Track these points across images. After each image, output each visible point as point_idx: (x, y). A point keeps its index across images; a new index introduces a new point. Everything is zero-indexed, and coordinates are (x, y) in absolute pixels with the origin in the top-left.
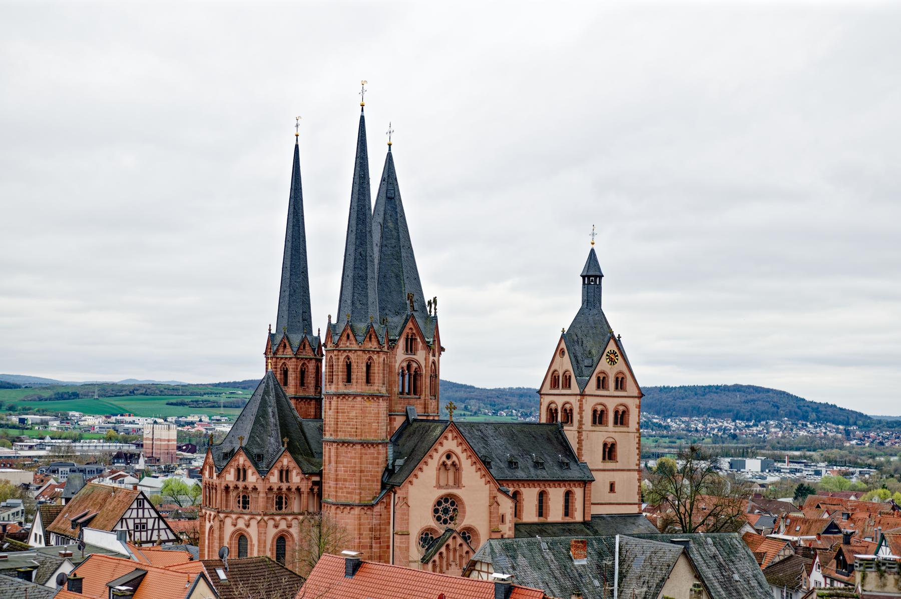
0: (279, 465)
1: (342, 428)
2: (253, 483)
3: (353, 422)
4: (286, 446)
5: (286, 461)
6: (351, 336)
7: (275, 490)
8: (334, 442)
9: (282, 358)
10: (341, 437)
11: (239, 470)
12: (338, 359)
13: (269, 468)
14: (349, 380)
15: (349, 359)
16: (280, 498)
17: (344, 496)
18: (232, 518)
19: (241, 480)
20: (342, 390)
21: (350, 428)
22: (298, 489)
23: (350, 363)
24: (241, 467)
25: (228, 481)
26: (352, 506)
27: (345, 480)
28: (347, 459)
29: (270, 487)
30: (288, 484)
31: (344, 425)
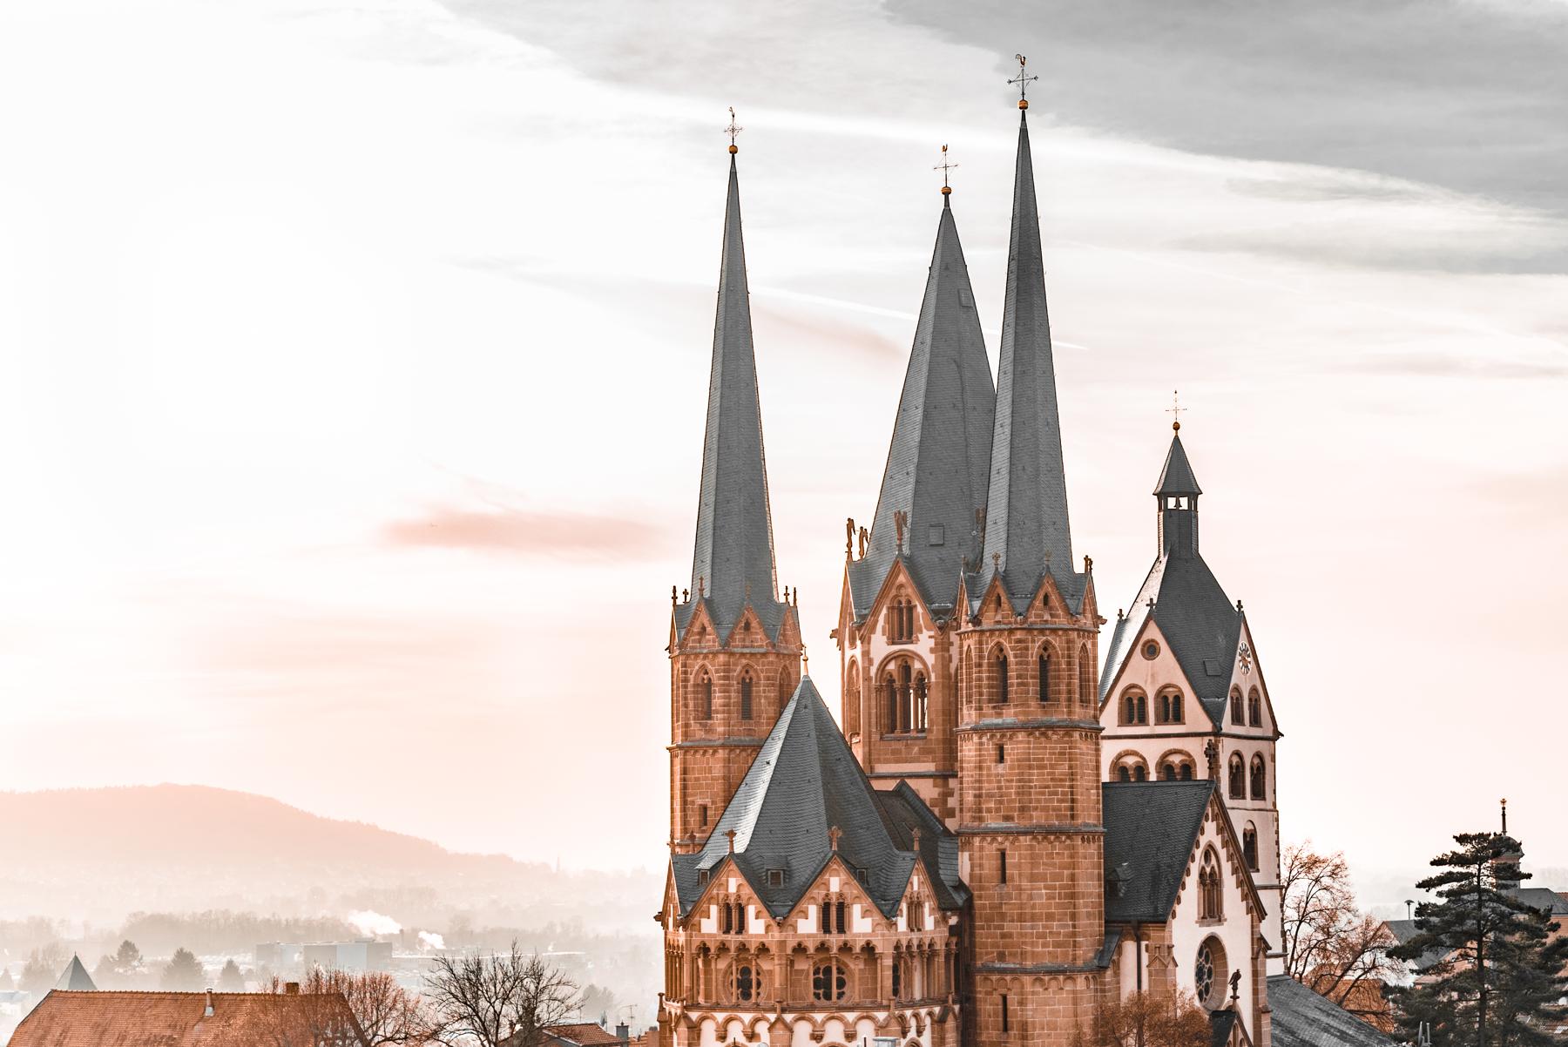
0: (818, 893)
1: (1038, 801)
2: (865, 935)
3: (1063, 786)
4: (835, 848)
5: (836, 883)
6: (1054, 600)
7: (811, 950)
8: (1025, 833)
9: (743, 655)
10: (1037, 818)
11: (728, 908)
12: (1027, 649)
13: (798, 897)
14: (1044, 696)
15: (1002, 650)
16: (828, 971)
17: (1049, 953)
18: (742, 1022)
19: (733, 932)
20: (1035, 712)
21: (1059, 801)
22: (869, 949)
23: (1005, 657)
24: (834, 900)
25: (803, 936)
26: (1068, 973)
27: (1050, 917)
28: (1051, 870)
29: (799, 945)
30: (843, 937)
31: (1043, 794)
